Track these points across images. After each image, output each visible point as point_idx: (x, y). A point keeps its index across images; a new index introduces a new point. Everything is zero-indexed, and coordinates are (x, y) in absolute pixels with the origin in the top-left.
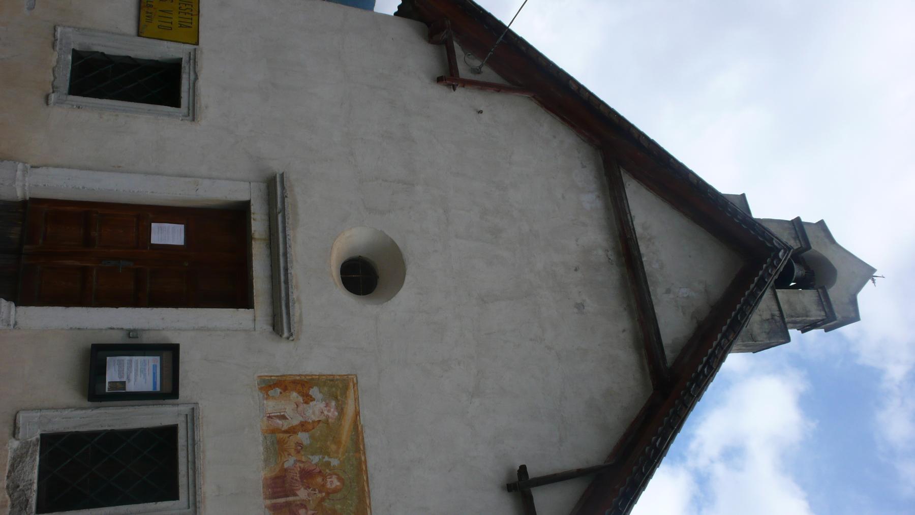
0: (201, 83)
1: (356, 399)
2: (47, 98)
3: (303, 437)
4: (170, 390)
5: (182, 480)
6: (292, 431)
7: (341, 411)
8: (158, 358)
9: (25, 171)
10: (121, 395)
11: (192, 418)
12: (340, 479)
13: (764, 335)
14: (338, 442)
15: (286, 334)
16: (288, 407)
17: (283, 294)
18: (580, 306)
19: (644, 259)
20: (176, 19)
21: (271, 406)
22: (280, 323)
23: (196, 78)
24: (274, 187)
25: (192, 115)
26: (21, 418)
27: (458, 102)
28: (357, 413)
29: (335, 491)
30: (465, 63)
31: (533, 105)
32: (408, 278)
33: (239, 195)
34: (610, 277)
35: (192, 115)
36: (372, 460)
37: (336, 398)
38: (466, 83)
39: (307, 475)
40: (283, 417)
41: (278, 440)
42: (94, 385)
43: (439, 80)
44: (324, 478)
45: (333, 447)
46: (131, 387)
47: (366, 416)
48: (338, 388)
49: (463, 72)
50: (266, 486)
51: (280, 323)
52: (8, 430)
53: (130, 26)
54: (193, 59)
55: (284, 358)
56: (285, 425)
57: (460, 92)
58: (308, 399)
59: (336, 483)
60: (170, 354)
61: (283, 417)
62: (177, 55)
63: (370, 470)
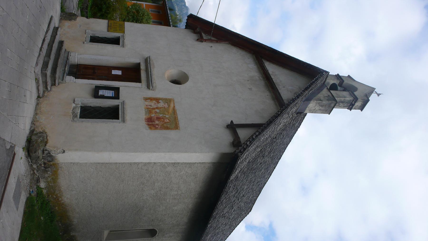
0: (125, 41)
1: (174, 104)
2: (84, 43)
3: (157, 111)
4: (117, 97)
5: (120, 116)
6: (154, 109)
7: (169, 106)
8: (114, 91)
9: (78, 55)
10: (103, 97)
11: (123, 103)
12: (169, 120)
13: (323, 96)
14: (168, 113)
15: (151, 87)
16: (153, 104)
17: (150, 73)
18: (250, 89)
19: (273, 80)
20: (118, 29)
21: (147, 103)
22: (149, 85)
23: (124, 39)
24: (147, 61)
25: (123, 46)
26: (76, 100)
27: (205, 46)
28: (174, 107)
29: (168, 122)
30: (205, 36)
31: (229, 46)
32: (190, 78)
33: (137, 61)
34: (262, 83)
35: (123, 46)
36: (179, 117)
37: (167, 103)
38: (206, 40)
39: (158, 119)
40: (151, 106)
41: (149, 110)
42: (95, 94)
43: (197, 40)
44: (164, 119)
45: (167, 113)
46: (106, 95)
47: (177, 107)
48: (168, 101)
49: (205, 38)
50: (145, 119)
51: (149, 85)
52: (72, 102)
53: (106, 30)
54: (123, 36)
55: (150, 94)
56: (152, 108)
57: (204, 43)
58: (158, 102)
59: (168, 121)
60: (117, 90)
61: (151, 106)
62: (119, 36)
63: (179, 119)
